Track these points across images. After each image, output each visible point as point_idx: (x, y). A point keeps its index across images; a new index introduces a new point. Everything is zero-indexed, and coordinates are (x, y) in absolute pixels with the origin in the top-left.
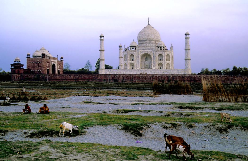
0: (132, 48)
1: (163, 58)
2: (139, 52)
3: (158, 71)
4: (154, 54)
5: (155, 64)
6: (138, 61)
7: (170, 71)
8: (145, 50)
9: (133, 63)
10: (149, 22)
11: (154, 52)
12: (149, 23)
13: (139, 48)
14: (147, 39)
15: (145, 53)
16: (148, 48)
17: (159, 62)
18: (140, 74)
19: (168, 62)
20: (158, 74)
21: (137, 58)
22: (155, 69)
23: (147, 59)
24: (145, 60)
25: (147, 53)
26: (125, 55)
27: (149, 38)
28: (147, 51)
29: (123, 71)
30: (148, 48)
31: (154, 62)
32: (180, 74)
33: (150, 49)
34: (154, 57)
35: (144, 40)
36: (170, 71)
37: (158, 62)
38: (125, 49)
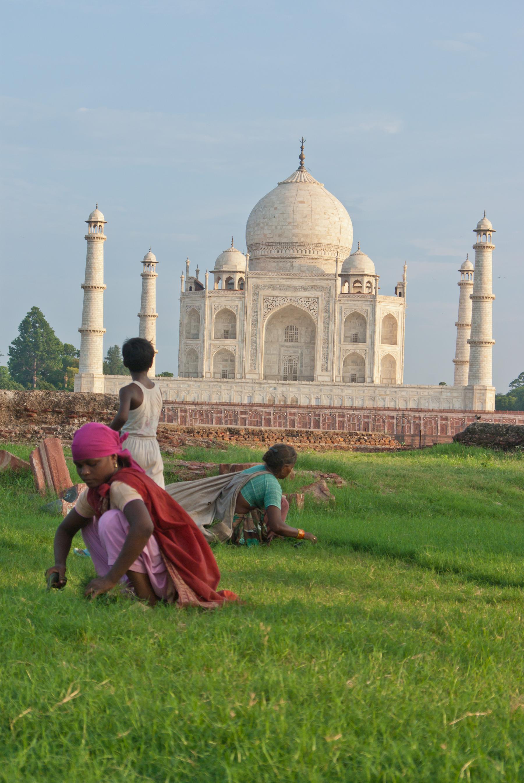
0: (225, 277)
1: (369, 332)
2: (261, 300)
3: (348, 391)
4: (327, 311)
5: (330, 356)
6: (254, 343)
7: (404, 393)
8: (288, 293)
9: (226, 350)
10: (301, 157)
11: (329, 302)
12: (301, 163)
13: (259, 282)
14: (295, 240)
15: (287, 303)
16: (302, 283)
17: (351, 347)
18: (266, 402)
19: (389, 349)
20: (347, 403)
21: (249, 329)
22: (328, 379)
23: (291, 335)
24: (282, 338)
25: (295, 304)
26: (193, 309)
27: (306, 236)
28: (295, 294)
29: (189, 386)
30: (302, 283)
31: (328, 348)
32: (445, 406)
33: (313, 288)
34: (327, 324)
35: (280, 243)
36: (404, 393)
37: (345, 351)
38: (189, 278)
